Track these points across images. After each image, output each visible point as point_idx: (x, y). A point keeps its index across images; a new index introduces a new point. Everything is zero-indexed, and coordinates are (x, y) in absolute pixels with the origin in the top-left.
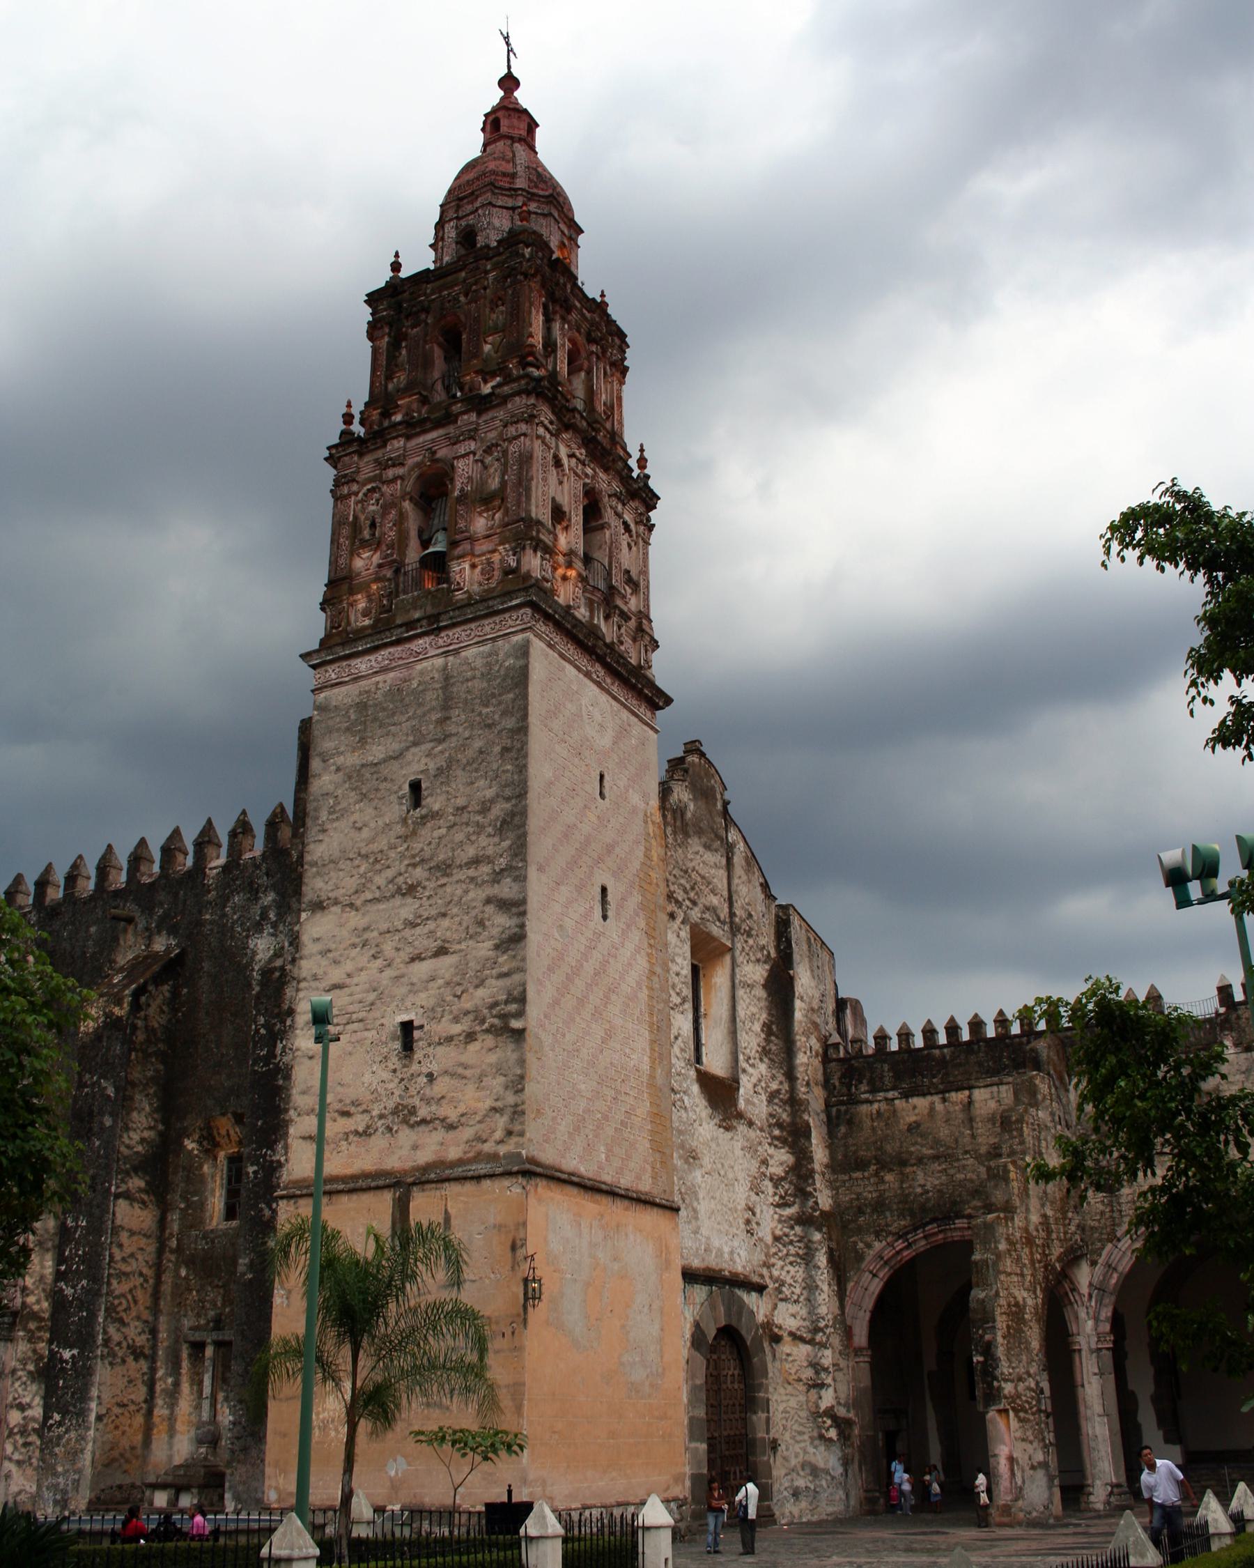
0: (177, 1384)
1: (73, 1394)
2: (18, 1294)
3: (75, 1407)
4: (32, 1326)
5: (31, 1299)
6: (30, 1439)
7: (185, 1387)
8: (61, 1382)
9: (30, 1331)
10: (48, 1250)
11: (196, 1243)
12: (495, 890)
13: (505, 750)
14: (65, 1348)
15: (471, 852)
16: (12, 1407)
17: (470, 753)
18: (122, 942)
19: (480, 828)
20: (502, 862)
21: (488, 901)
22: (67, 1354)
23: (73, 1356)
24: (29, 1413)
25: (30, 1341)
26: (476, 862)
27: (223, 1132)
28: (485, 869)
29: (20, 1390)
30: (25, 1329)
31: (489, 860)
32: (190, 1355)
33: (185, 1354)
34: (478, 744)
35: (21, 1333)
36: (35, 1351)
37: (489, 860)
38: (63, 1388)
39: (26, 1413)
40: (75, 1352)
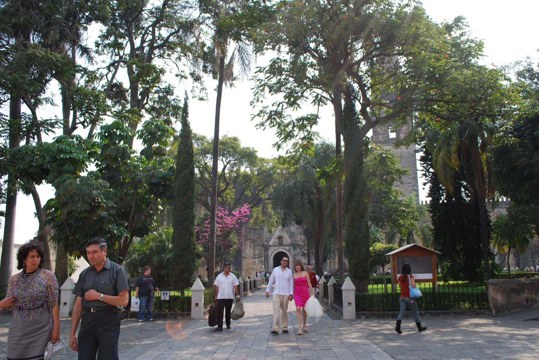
0: (335, 256)
4: (300, 247)
5: (299, 243)
12: (413, 188)
13: (413, 167)
15: (408, 181)
17: (406, 166)
19: (409, 178)
20: (414, 184)
21: (412, 189)
26: (409, 183)
28: (411, 185)
31: (412, 183)
34: (408, 165)
37: (412, 183)
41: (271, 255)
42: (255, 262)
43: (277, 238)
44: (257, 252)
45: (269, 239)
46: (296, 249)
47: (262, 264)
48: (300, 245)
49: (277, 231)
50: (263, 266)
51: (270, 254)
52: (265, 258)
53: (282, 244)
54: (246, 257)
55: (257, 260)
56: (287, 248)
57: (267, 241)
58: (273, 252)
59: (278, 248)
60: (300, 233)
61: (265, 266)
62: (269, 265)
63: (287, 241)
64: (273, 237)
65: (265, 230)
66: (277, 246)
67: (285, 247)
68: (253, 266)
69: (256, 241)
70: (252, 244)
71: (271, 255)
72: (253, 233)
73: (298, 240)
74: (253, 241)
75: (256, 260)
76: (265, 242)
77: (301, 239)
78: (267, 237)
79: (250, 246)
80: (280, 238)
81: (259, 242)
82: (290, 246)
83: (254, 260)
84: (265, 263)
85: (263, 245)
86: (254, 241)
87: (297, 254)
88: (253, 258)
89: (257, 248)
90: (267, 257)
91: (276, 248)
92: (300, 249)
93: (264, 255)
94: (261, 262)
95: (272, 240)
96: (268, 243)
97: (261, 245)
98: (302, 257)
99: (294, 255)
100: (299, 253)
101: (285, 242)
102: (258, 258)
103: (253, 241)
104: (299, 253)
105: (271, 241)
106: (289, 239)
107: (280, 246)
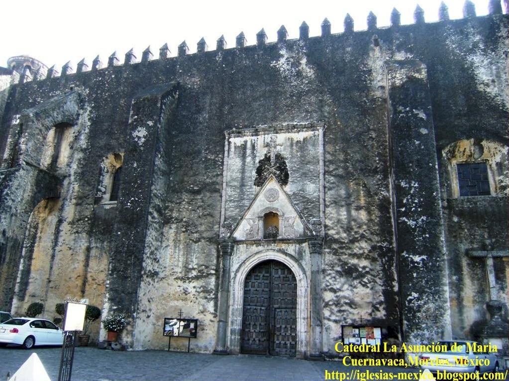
0: (460, 280)
1: (427, 282)
2: (323, 228)
3: (430, 289)
4: (335, 246)
5: (331, 232)
6: (343, 308)
7: (467, 281)
8: (415, 275)
9: (335, 249)
10: (342, 206)
11: (463, 204)
14: (414, 255)
16: (326, 290)
18: (371, 55)
22: (417, 259)
23: (423, 260)
24: (340, 294)
25: (335, 254)
27: (462, 150)
29: (330, 281)
30: (330, 247)
32: (468, 264)
33: (464, 262)
35: (327, 250)
36: (340, 260)
38: (417, 278)
39: (338, 294)
40: (424, 257)
41: (237, 271)
42: (186, 292)
43: (260, 217)
44: (195, 261)
45: (234, 219)
46: (320, 253)
47: (209, 300)
48: (336, 241)
49: (261, 197)
50: (211, 306)
51: (234, 268)
52: (217, 278)
53: (275, 236)
54: (161, 275)
55: (192, 285)
56: (292, 249)
57: (228, 227)
58: (244, 262)
59: (260, 248)
60: (335, 203)
61: (216, 305)
62: (231, 302)
63: (292, 226)
64: (248, 215)
65: (224, 193)
66: (257, 243)
67: (283, 246)
68: (180, 304)
69: (196, 226)
70: (182, 236)
71: (237, 271)
72: (189, 203)
73: (329, 223)
74: (187, 225)
75: (191, 286)
76: (222, 229)
77: (339, 221)
78: (229, 213)
79: (176, 241)
80: (270, 217)
81: (203, 228)
82: (299, 241)
83: (186, 285)
84: (216, 294)
85: (214, 240)
86: (188, 227)
87: (324, 271)
88: (182, 279)
89: (195, 246)
90: (224, 276)
91: (254, 248)
92: (335, 253)
93: (217, 270)
94: (206, 291)
95: (244, 222)
96: (232, 233)
97: (210, 240)
98: (343, 280)
99: (315, 273)
100: (332, 266)
101: (283, 232)
102: (197, 278)
103: (187, 225)
104: (332, 266)
105: (241, 227)
106: (298, 220)
107: (269, 243)
